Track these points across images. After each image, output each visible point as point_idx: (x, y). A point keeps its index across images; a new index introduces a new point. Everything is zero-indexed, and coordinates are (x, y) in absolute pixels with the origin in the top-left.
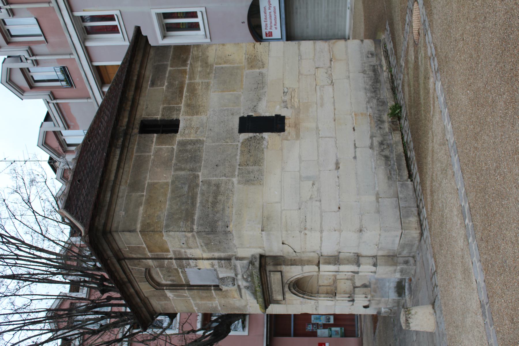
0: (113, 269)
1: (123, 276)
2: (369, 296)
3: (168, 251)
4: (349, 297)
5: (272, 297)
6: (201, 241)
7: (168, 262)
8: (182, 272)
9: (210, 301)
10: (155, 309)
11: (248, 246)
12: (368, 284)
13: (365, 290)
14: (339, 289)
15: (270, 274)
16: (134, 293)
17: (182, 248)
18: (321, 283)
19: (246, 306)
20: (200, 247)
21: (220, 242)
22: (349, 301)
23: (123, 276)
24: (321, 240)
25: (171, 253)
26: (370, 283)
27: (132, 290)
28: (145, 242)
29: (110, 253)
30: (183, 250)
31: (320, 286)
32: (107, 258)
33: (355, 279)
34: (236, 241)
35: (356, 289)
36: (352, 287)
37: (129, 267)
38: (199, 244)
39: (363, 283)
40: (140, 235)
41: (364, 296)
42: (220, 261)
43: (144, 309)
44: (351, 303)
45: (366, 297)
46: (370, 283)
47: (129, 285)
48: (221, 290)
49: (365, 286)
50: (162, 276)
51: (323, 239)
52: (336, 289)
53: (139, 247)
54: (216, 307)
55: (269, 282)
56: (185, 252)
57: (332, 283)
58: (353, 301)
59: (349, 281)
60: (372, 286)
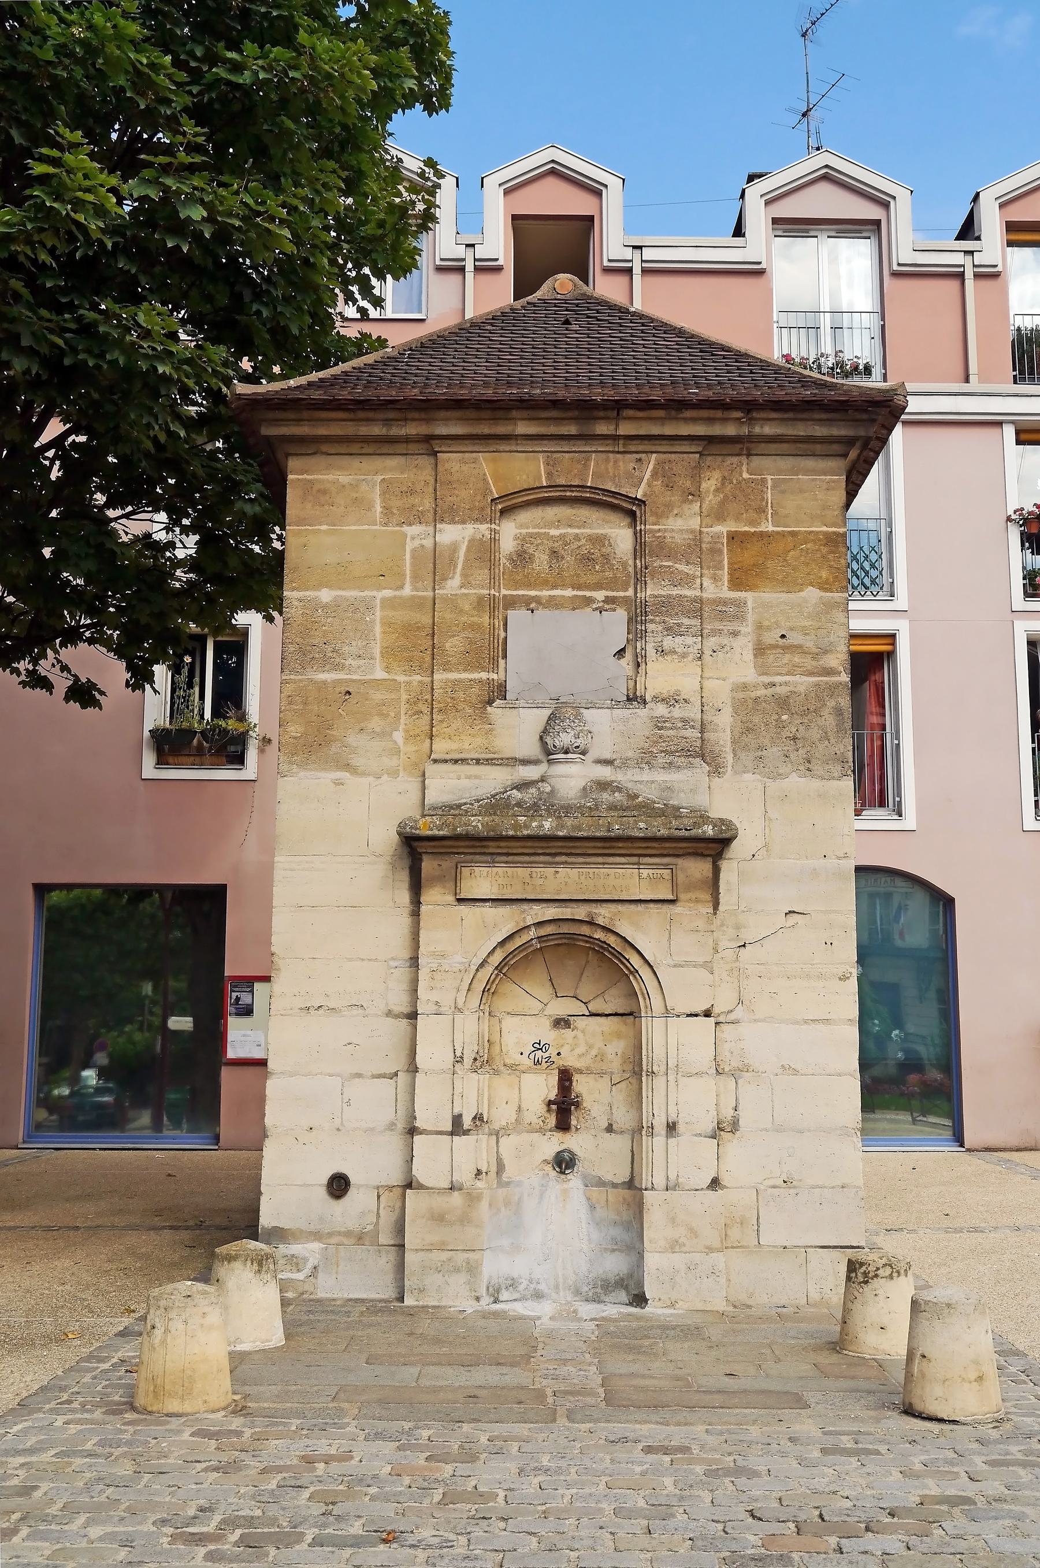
0: (688, 414)
1: (626, 428)
2: (479, 1184)
3: (737, 582)
4: (478, 1118)
5: (492, 864)
6: (802, 689)
7: (694, 577)
8: (589, 601)
9: (388, 653)
10: (320, 461)
11: (770, 814)
12: (505, 1178)
13: (494, 1169)
14: (497, 1081)
15: (666, 866)
16: (501, 429)
17: (759, 627)
18: (509, 1023)
19: (347, 767)
20: (767, 679)
21: (794, 739)
22: (457, 1120)
23: (626, 428)
24: (806, 1022)
25: (726, 593)
26: (508, 1184)
27: (523, 428)
28: (782, 534)
29: (768, 430)
30: (747, 629)
31: (500, 1022)
32: (755, 414)
33: (520, 1133)
34: (795, 782)
35: (494, 1137)
36: (496, 1126)
37: (654, 455)
38: (778, 679)
39: (506, 1162)
40: (825, 529)
41: (484, 1170)
42: (698, 725)
43: (377, 430)
44: (449, 1127)
45: (479, 1172)
46: (508, 1184)
47: (572, 429)
48: (490, 702)
49: (500, 1168)
50: (554, 532)
51: (820, 1027)
52: (496, 1072)
53: (762, 510)
54: (337, 667)
55: (611, 859)
56: (735, 634)
57: (508, 1061)
58: (457, 1128)
59: (514, 1117)
60: (502, 1192)
